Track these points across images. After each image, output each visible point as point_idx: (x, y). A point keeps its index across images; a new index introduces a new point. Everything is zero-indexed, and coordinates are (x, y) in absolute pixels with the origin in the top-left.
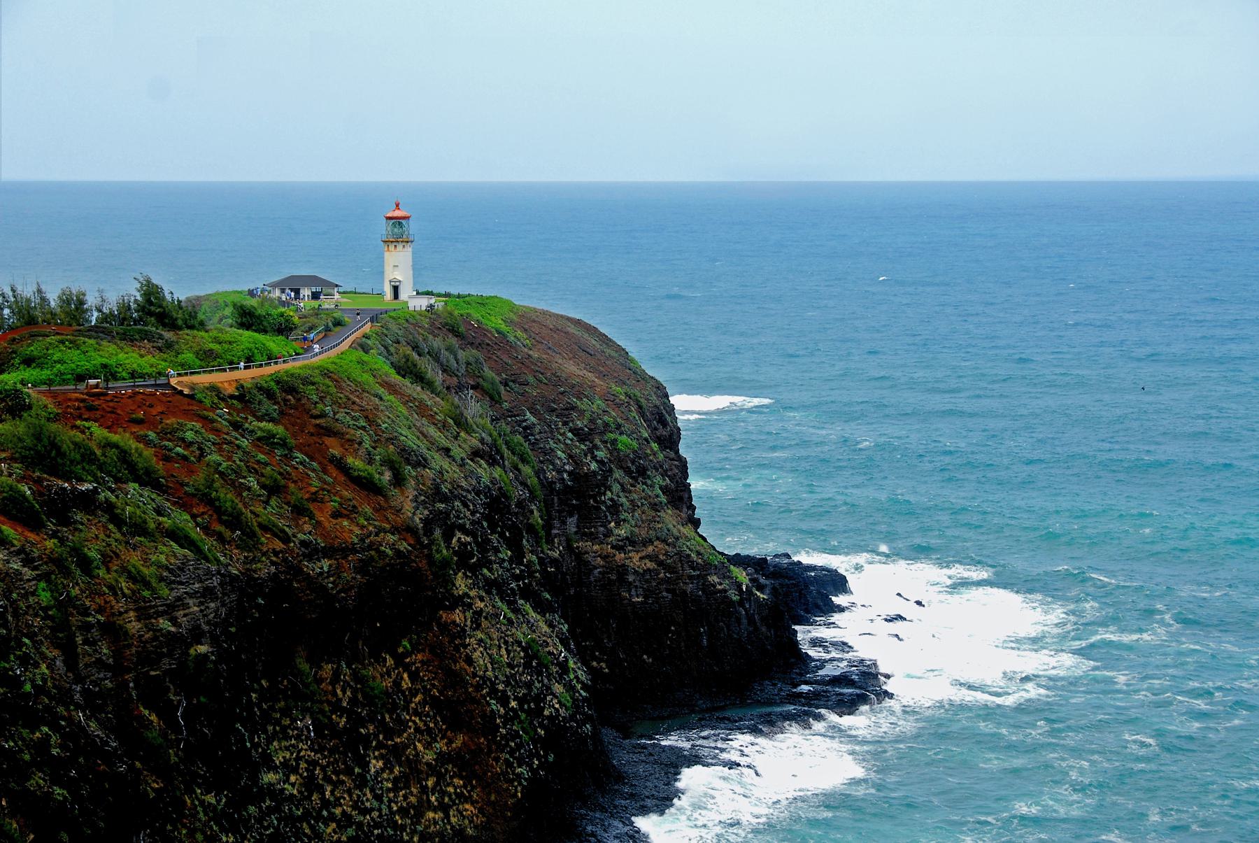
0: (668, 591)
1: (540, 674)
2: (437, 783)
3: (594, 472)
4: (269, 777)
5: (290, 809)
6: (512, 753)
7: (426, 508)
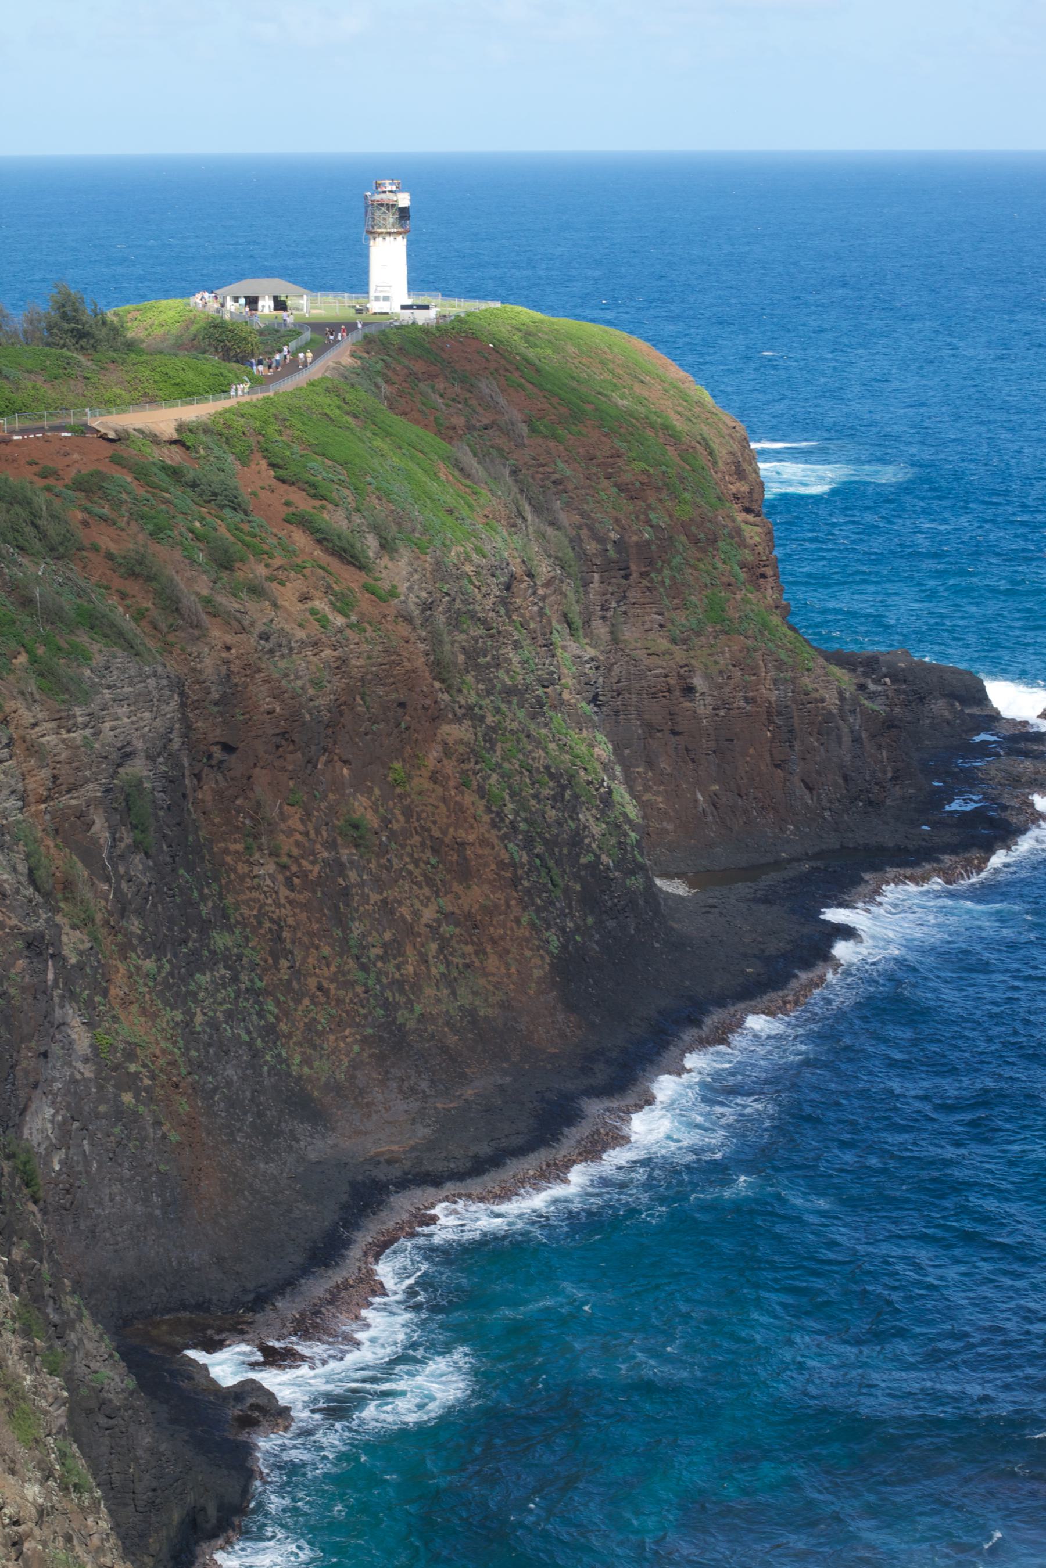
2: (441, 949)
3: (648, 543)
4: (221, 940)
5: (251, 981)
6: (538, 910)
7: (425, 589)
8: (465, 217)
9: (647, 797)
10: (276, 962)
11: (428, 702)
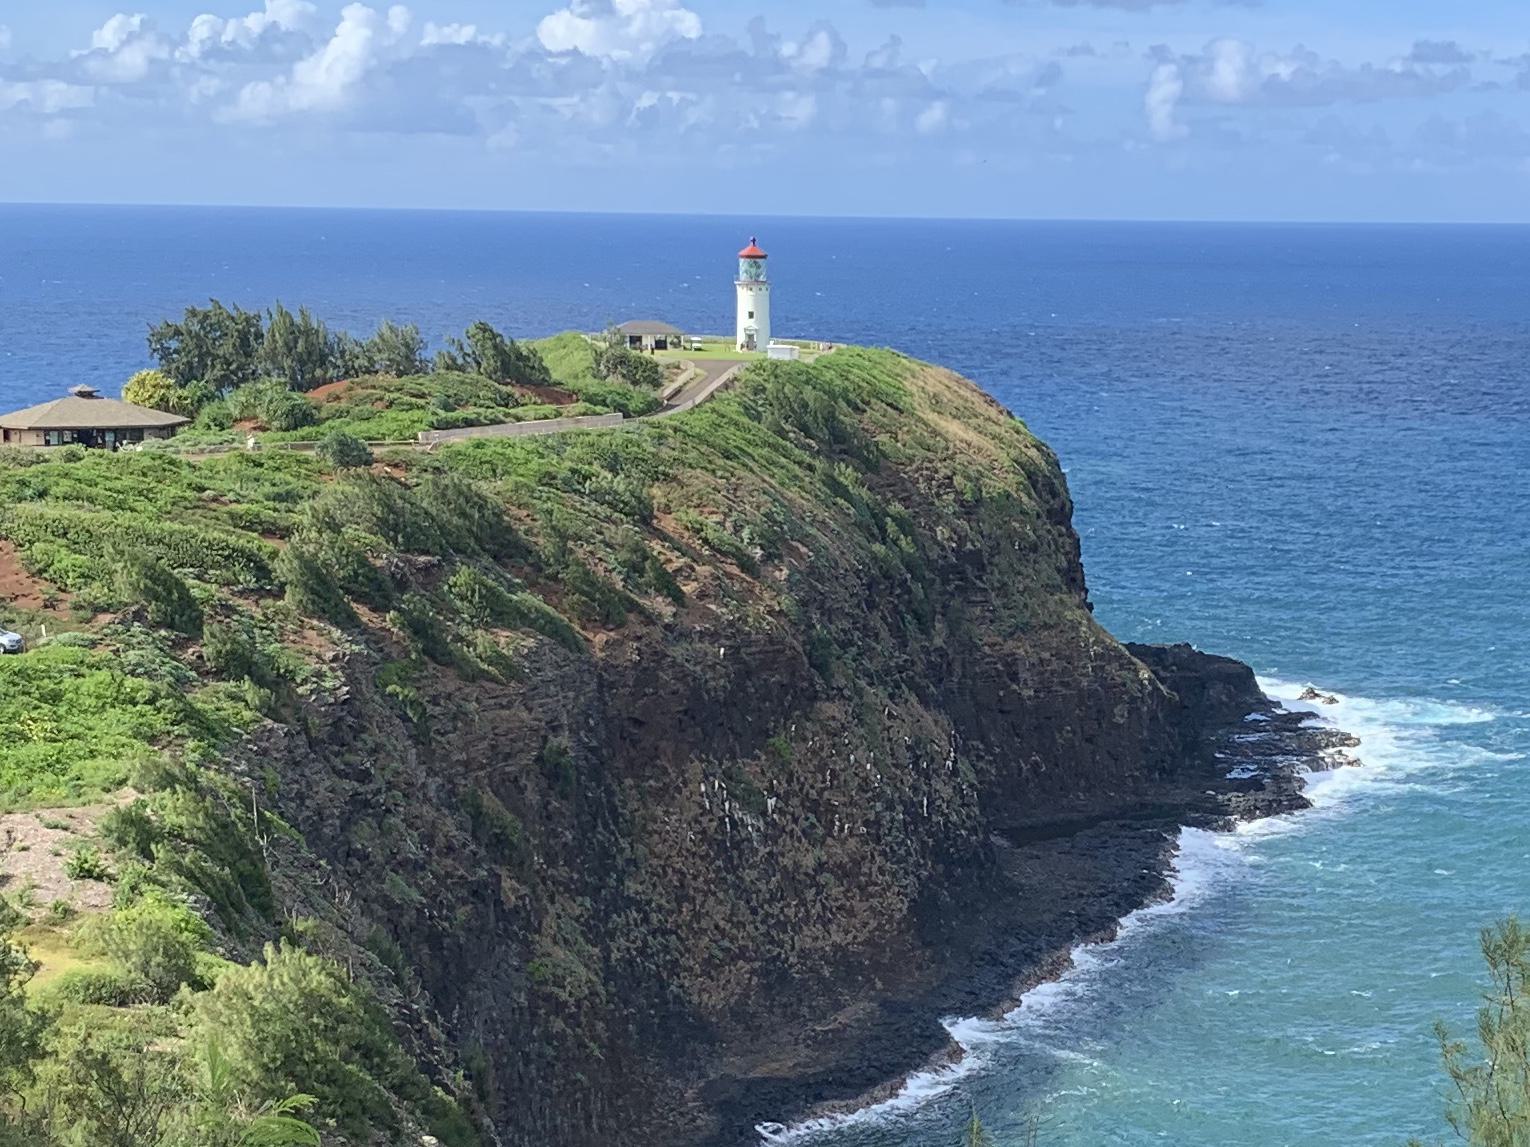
0: (1062, 683)
1: (928, 778)
4: (632, 887)
8: (816, 271)
9: (981, 764)
10: (680, 906)
11: (805, 684)
